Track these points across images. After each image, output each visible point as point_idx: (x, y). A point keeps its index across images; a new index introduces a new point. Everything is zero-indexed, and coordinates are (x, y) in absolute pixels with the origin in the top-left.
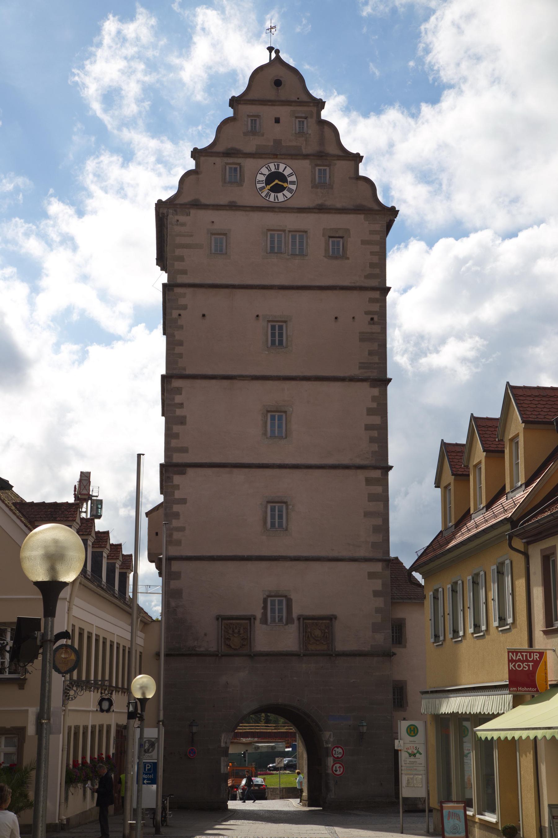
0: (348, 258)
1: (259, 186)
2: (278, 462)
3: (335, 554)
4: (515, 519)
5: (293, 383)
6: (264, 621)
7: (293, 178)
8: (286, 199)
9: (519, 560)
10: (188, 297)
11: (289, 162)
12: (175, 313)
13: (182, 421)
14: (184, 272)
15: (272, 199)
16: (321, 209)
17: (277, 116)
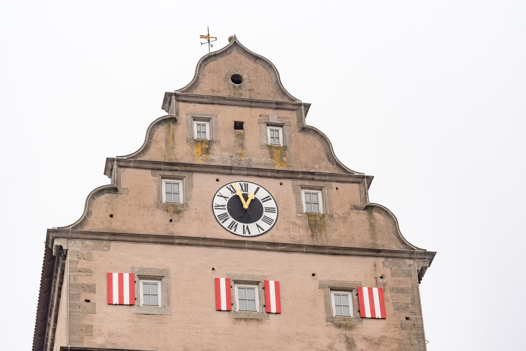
1: (218, 212)
7: (271, 204)
8: (262, 232)
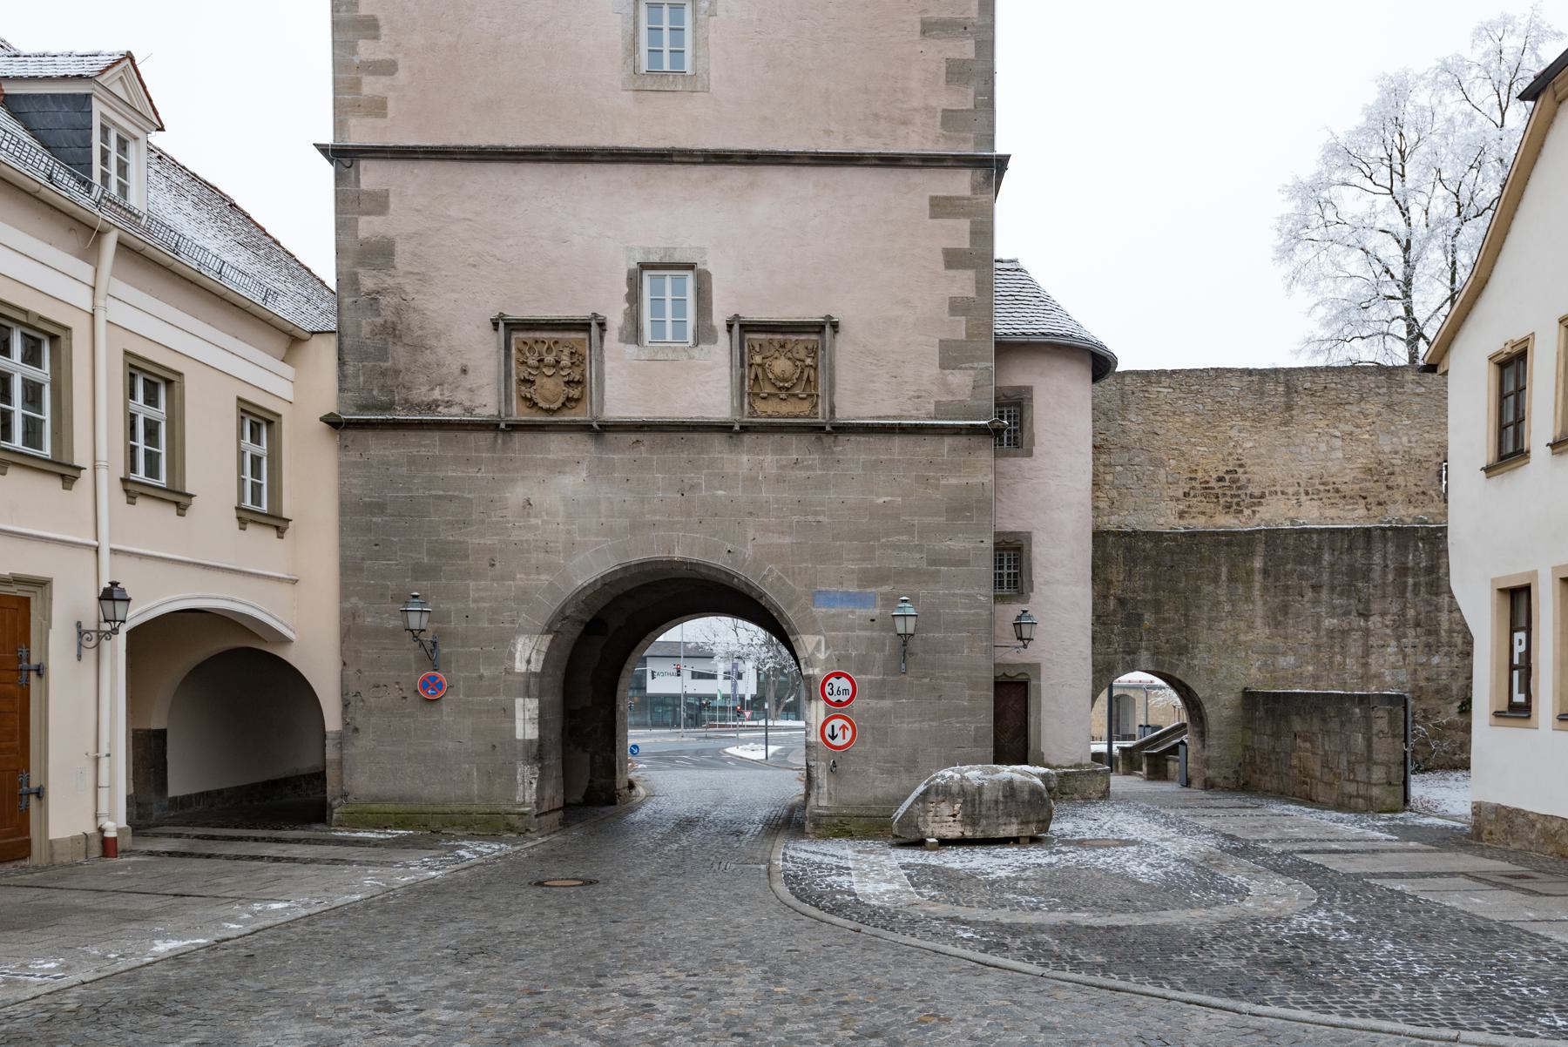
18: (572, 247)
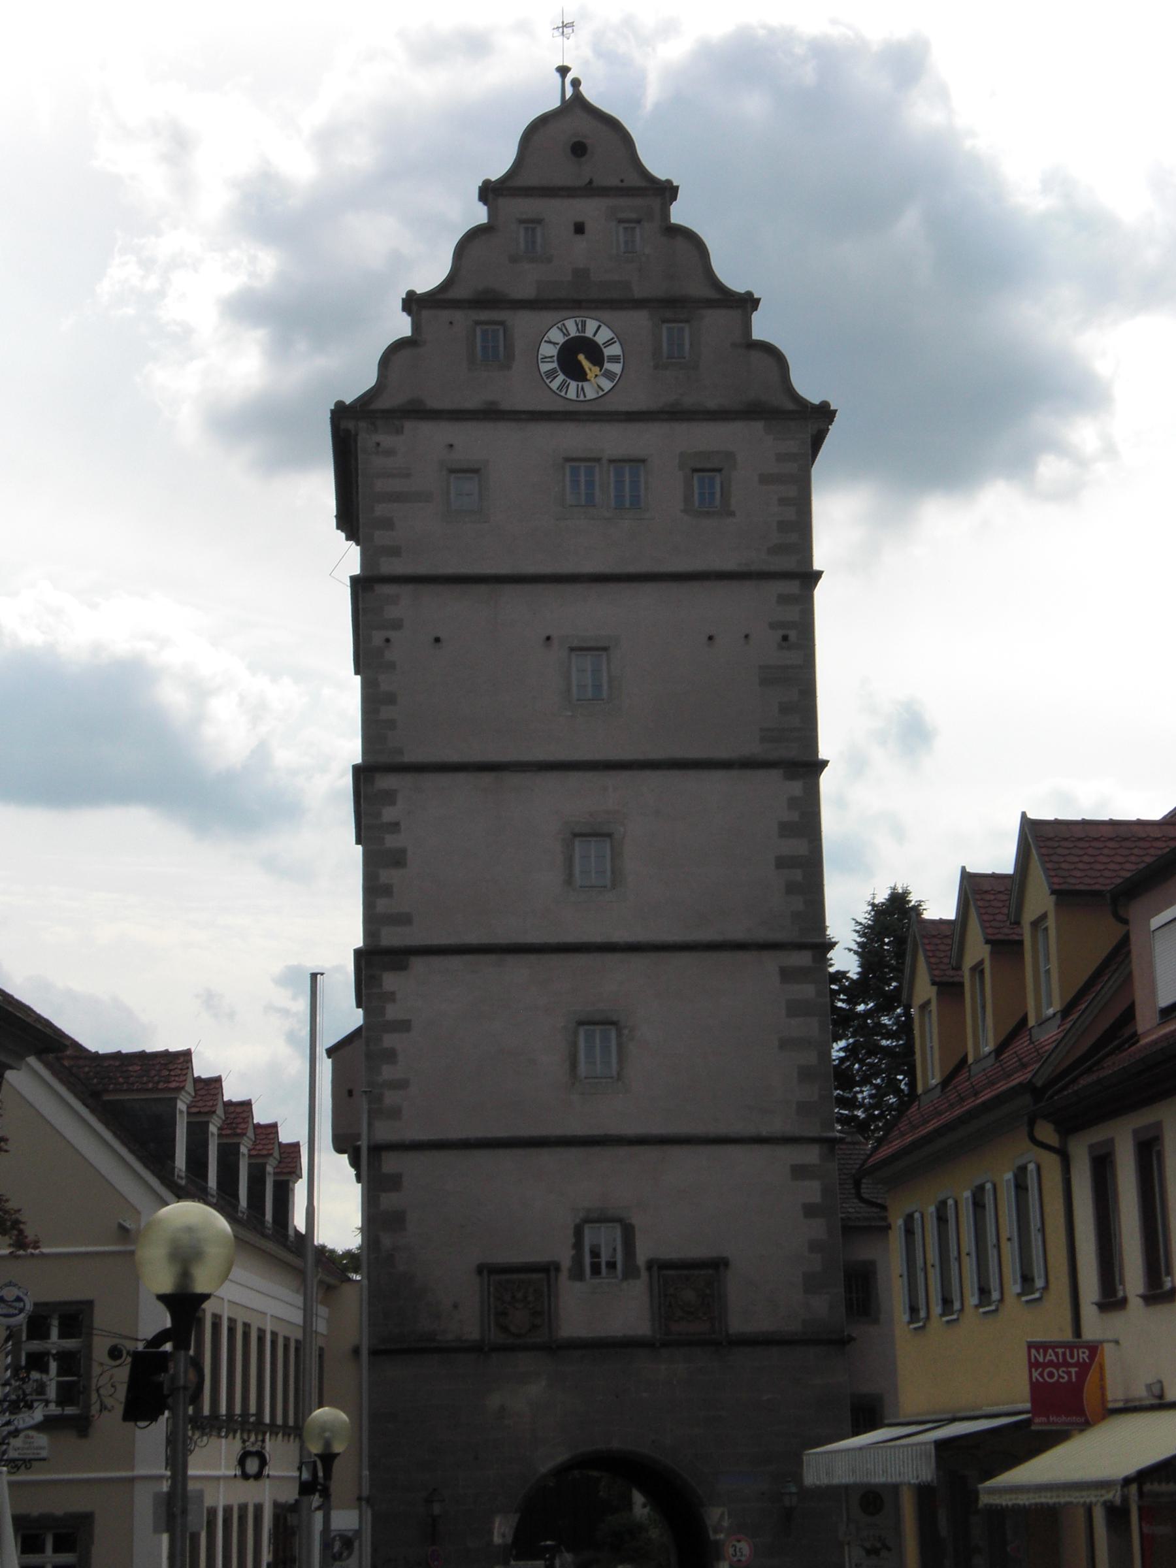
0: (732, 514)
1: (545, 367)
2: (598, 939)
3: (722, 1129)
4: (1039, 1084)
5: (625, 775)
6: (577, 1274)
7: (615, 350)
8: (601, 393)
9: (1051, 1162)
10: (402, 604)
11: (606, 315)
12: (378, 638)
13: (398, 859)
14: (395, 551)
15: (572, 394)
16: (674, 414)
17: (579, 219)
18: (534, 1207)
